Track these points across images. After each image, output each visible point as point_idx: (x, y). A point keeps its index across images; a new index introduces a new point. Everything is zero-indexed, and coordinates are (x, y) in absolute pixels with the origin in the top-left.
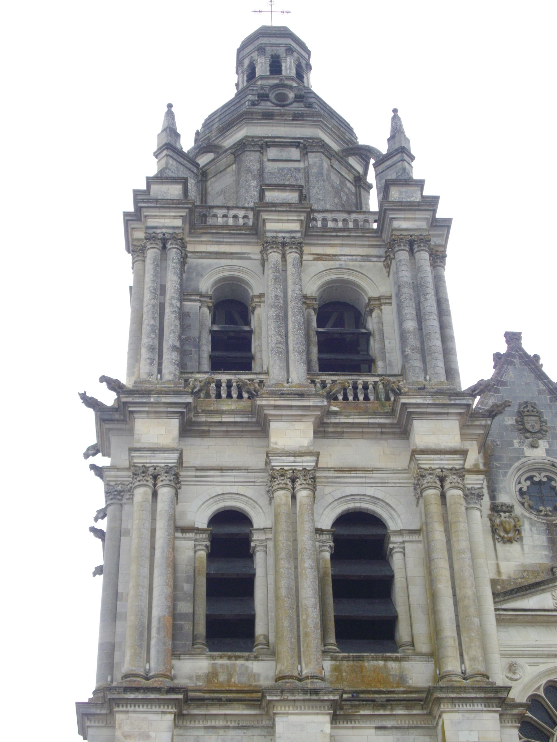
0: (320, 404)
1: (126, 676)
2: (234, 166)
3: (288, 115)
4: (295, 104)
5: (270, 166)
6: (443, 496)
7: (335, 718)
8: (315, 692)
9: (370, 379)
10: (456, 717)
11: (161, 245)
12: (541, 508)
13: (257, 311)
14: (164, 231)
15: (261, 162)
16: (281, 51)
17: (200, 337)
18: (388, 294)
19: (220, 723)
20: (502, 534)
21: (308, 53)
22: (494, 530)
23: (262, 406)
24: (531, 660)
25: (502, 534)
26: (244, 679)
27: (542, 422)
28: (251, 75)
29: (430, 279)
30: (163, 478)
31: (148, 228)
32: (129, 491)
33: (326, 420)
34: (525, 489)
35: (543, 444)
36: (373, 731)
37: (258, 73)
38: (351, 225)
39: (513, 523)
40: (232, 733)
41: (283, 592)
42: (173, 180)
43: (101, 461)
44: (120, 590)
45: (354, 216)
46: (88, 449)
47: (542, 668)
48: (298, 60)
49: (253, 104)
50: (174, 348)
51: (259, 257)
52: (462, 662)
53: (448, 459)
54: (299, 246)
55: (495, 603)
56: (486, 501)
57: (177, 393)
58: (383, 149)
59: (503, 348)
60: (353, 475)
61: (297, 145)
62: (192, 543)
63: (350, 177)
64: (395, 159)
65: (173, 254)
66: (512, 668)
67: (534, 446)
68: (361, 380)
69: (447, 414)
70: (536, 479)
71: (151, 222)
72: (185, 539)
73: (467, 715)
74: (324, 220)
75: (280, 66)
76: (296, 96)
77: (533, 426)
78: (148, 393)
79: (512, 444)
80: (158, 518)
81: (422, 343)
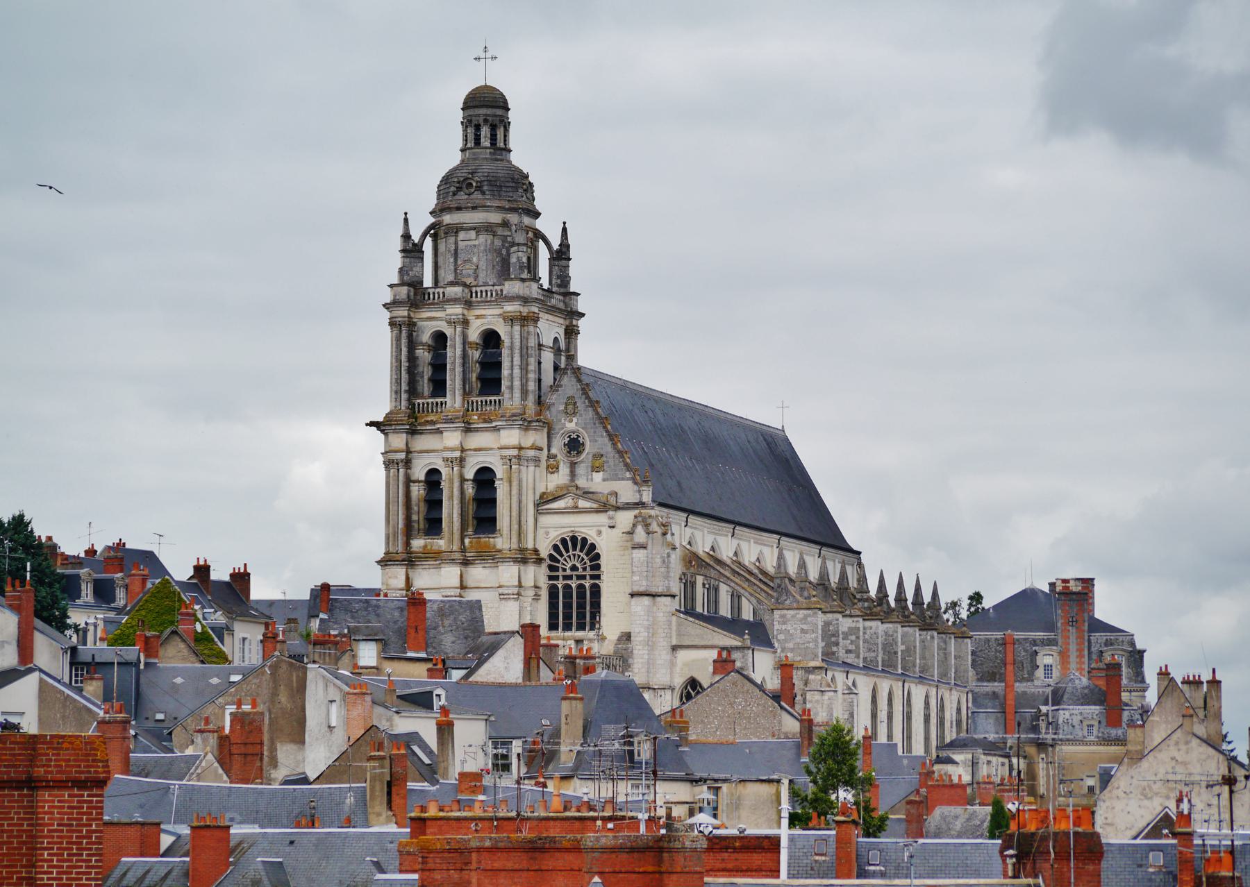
5: (460, 244)
14: (399, 319)
19: (427, 567)
26: (437, 548)
35: (575, 420)
40: (432, 570)
45: (496, 287)
47: (559, 533)
50: (406, 391)
67: (571, 421)
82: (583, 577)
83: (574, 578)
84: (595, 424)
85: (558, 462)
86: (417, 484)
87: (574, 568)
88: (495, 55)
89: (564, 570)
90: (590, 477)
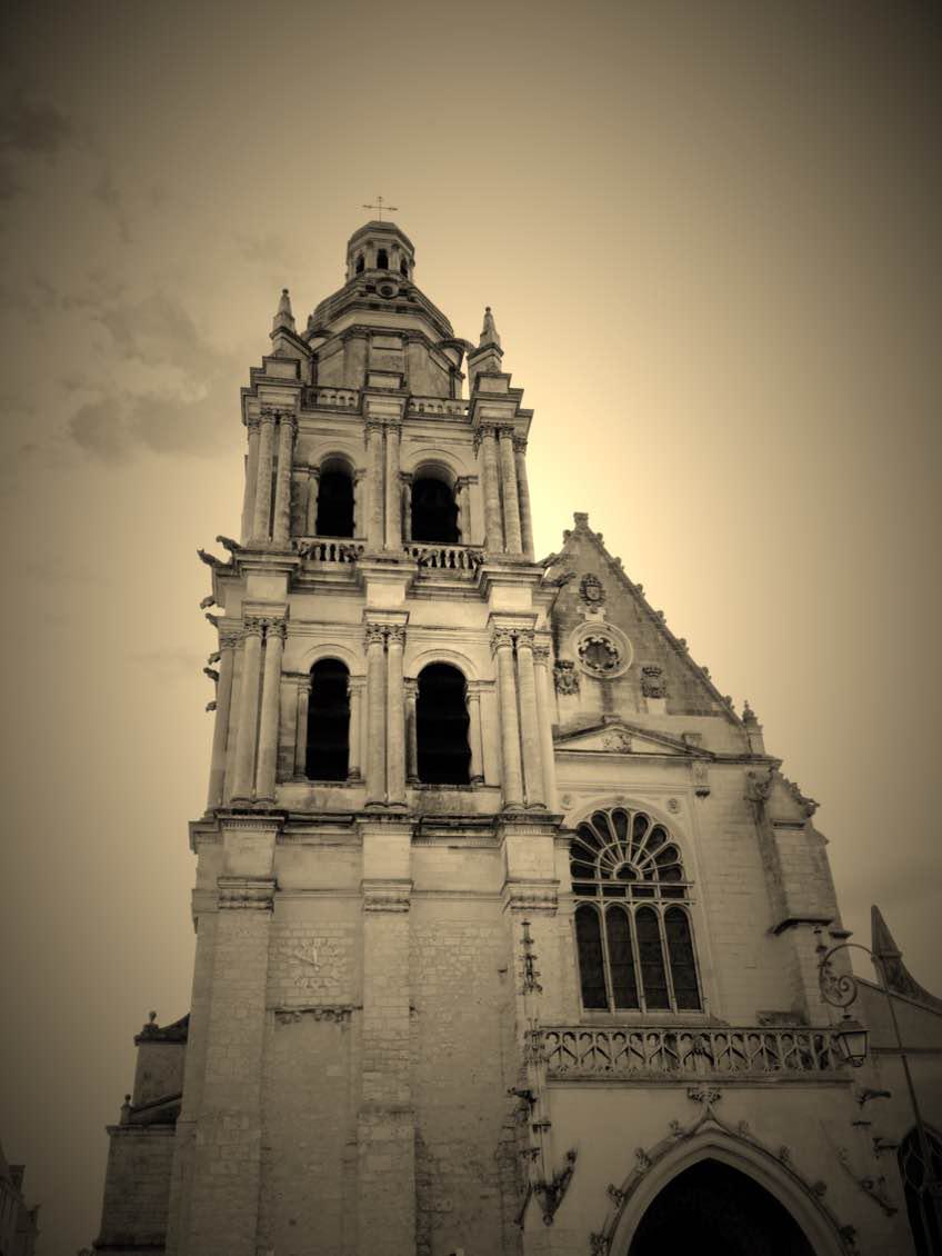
0: (411, 569)
1: (234, 800)
2: (342, 352)
3: (392, 308)
4: (399, 298)
5: (374, 353)
6: (515, 653)
7: (415, 838)
8: (398, 816)
9: (457, 550)
10: (518, 840)
11: (274, 421)
12: (597, 665)
13: (359, 484)
14: (278, 407)
15: (367, 349)
16: (388, 247)
17: (307, 506)
18: (475, 474)
20: (563, 686)
21: (413, 249)
22: (557, 683)
23: (360, 570)
24: (583, 794)
25: (563, 686)
27: (602, 592)
28: (360, 268)
29: (512, 463)
30: (272, 630)
31: (262, 403)
32: (241, 639)
33: (416, 584)
34: (584, 649)
35: (601, 611)
36: (446, 851)
37: (367, 265)
38: (445, 411)
39: (573, 677)
40: (326, 849)
41: (374, 731)
42: (288, 361)
43: (216, 611)
44: (232, 724)
45: (447, 403)
46: (205, 601)
47: (590, 800)
48: (403, 255)
49: (362, 295)
51: (362, 435)
52: (524, 793)
53: (522, 622)
54: (399, 428)
55: (555, 744)
56: (551, 658)
57: (286, 554)
58: (476, 343)
59: (572, 526)
60: (438, 632)
61: (399, 335)
62: (296, 686)
63: (446, 368)
64: (486, 353)
65: (286, 429)
66: (566, 799)
67: (593, 612)
68: (449, 549)
69: (522, 582)
70: (594, 641)
71: (266, 398)
72: (291, 683)
73: (526, 839)
74: (421, 405)
75: (387, 260)
76: (400, 290)
77: (594, 595)
78: (260, 553)
79: (575, 610)
80: (267, 663)
81: (503, 519)
82: (649, 892)
83: (629, 891)
84: (640, 620)
85: (576, 674)
86: (296, 679)
87: (626, 873)
88: (395, 206)
89: (606, 876)
90: (641, 705)
